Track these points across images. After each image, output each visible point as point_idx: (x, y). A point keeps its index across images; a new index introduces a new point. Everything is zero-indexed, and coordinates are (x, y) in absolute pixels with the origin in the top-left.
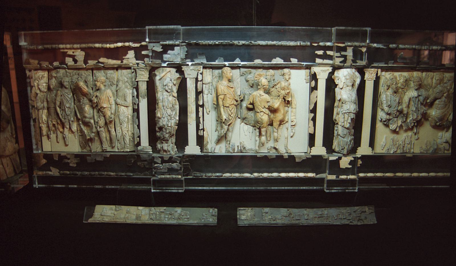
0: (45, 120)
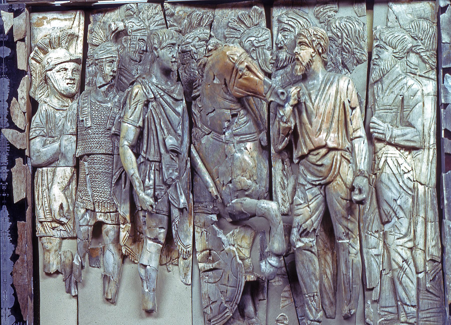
0: (61, 207)
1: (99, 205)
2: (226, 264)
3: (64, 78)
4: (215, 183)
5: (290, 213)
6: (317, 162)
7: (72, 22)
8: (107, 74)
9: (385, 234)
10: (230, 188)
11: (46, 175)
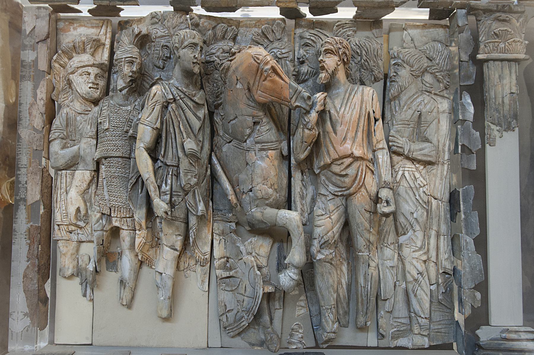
0: (78, 210)
1: (114, 210)
2: (244, 273)
4: (235, 191)
5: (308, 224)
6: (341, 172)
7: (99, 30)
8: (126, 75)
9: (400, 247)
10: (250, 196)
11: (65, 178)
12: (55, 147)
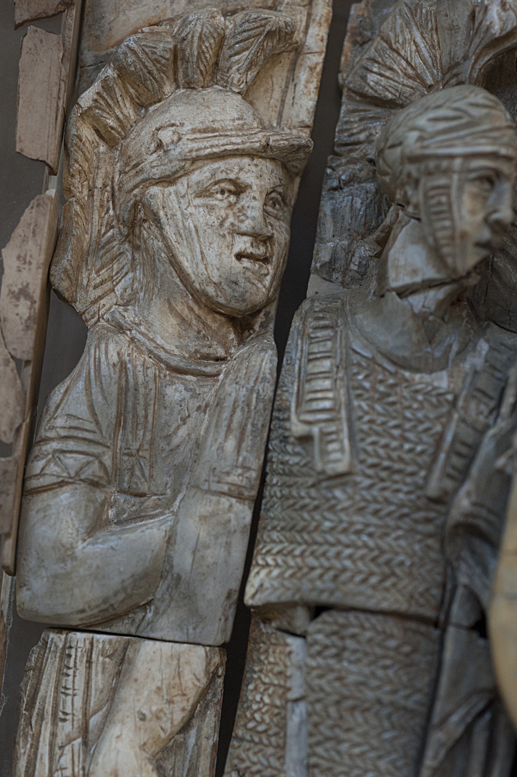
3: (227, 224)
8: (464, 235)
11: (82, 668)
12: (60, 518)
